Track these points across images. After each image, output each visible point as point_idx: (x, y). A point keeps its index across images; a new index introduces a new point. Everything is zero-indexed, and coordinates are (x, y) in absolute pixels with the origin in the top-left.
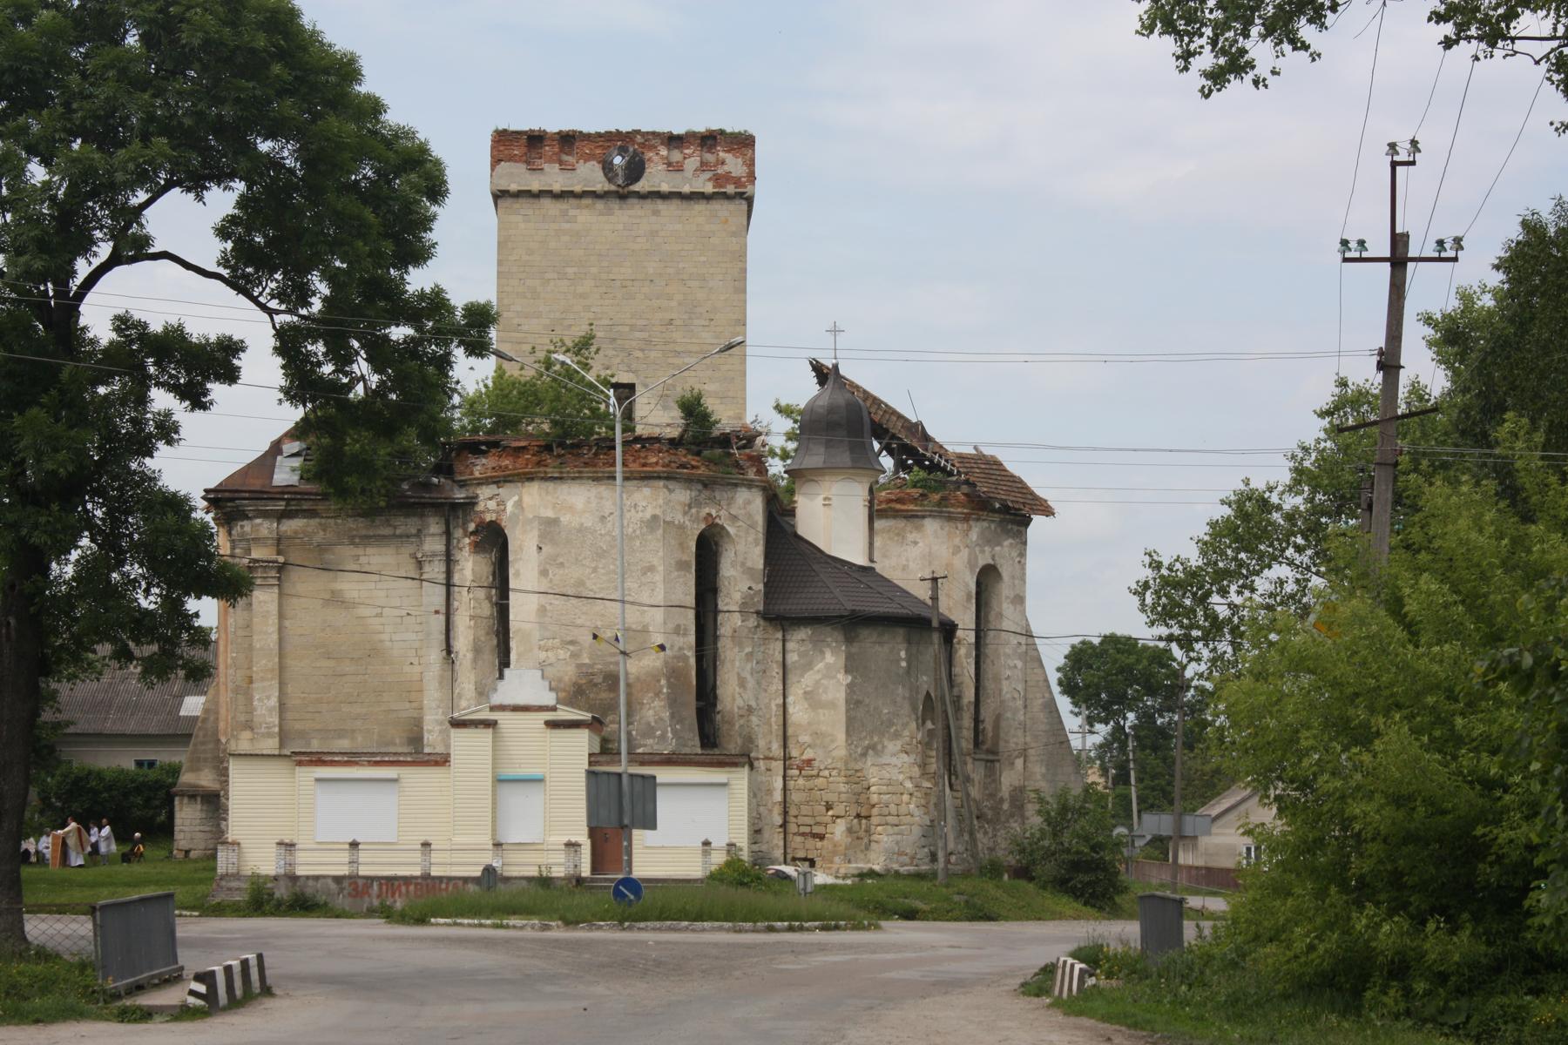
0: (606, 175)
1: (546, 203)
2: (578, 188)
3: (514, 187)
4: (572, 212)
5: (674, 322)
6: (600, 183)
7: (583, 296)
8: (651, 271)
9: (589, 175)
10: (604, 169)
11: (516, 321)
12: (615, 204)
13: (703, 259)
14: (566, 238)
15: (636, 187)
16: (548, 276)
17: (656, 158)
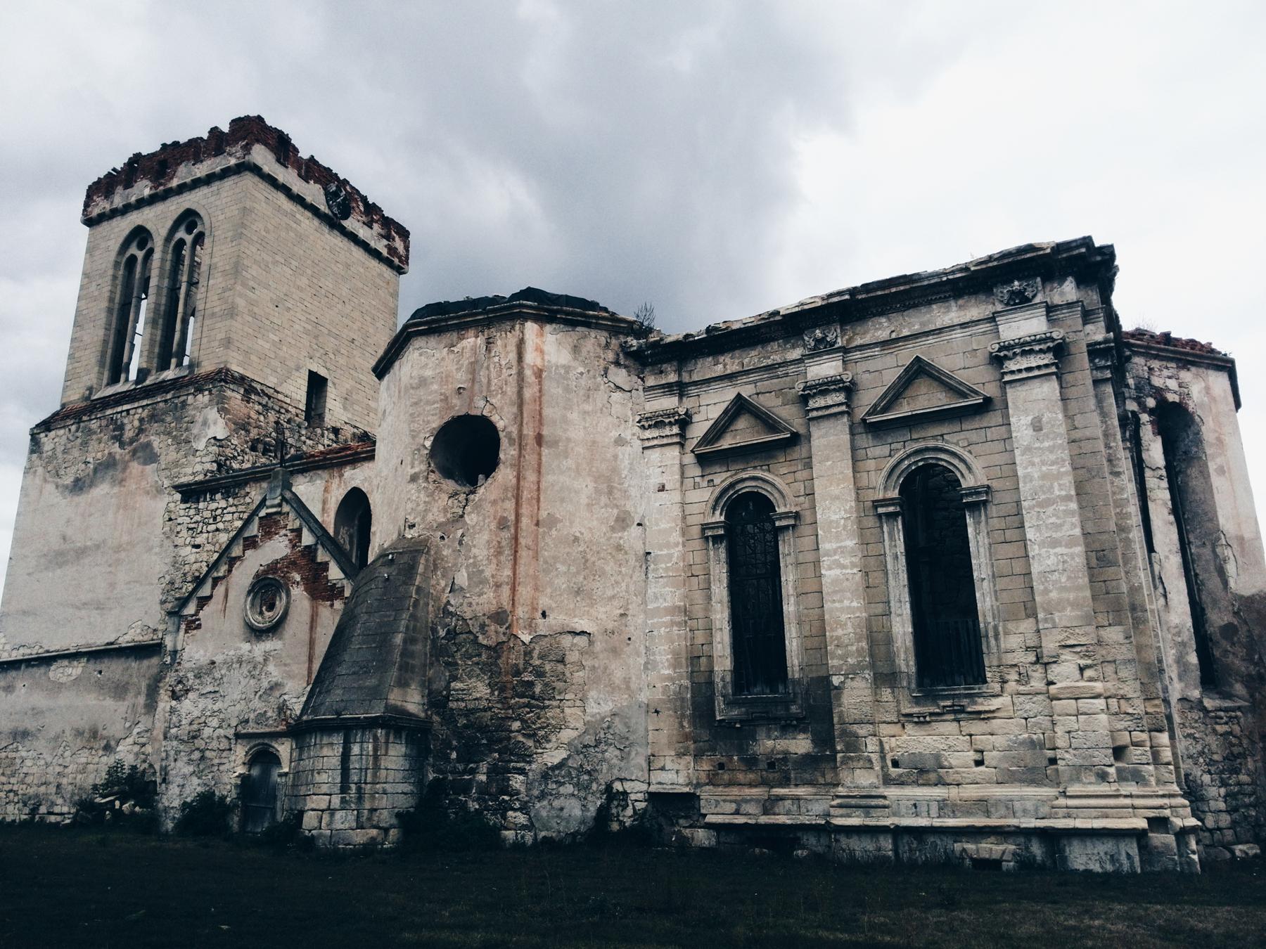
0: (327, 202)
1: (282, 199)
2: (309, 199)
3: (266, 169)
4: (298, 216)
5: (356, 342)
6: (323, 208)
7: (299, 288)
8: (344, 294)
9: (313, 192)
10: (326, 195)
11: (251, 283)
12: (326, 229)
13: (374, 303)
14: (292, 234)
15: (346, 223)
16: (278, 258)
17: (357, 210)
